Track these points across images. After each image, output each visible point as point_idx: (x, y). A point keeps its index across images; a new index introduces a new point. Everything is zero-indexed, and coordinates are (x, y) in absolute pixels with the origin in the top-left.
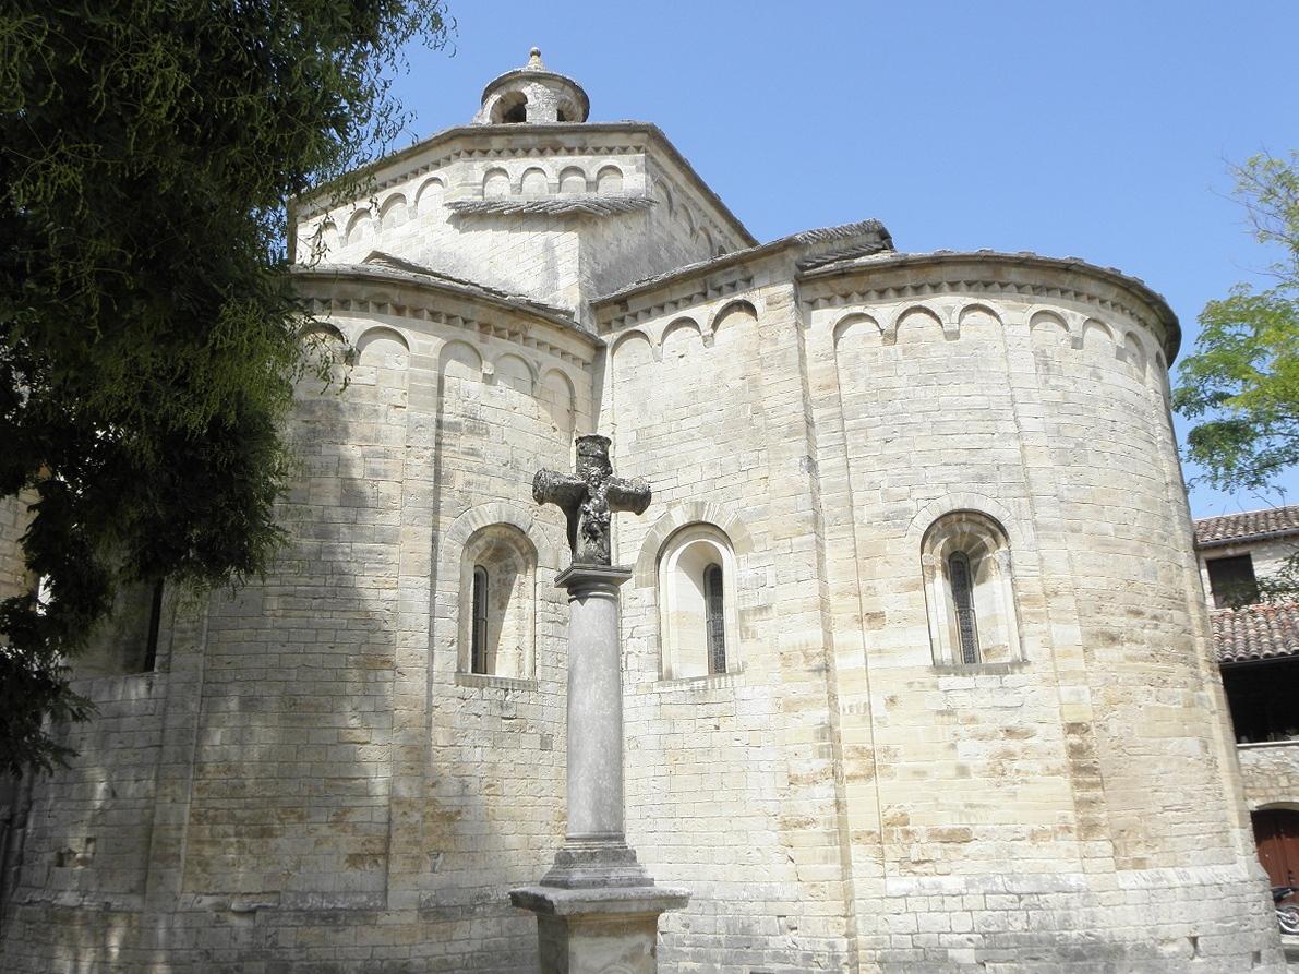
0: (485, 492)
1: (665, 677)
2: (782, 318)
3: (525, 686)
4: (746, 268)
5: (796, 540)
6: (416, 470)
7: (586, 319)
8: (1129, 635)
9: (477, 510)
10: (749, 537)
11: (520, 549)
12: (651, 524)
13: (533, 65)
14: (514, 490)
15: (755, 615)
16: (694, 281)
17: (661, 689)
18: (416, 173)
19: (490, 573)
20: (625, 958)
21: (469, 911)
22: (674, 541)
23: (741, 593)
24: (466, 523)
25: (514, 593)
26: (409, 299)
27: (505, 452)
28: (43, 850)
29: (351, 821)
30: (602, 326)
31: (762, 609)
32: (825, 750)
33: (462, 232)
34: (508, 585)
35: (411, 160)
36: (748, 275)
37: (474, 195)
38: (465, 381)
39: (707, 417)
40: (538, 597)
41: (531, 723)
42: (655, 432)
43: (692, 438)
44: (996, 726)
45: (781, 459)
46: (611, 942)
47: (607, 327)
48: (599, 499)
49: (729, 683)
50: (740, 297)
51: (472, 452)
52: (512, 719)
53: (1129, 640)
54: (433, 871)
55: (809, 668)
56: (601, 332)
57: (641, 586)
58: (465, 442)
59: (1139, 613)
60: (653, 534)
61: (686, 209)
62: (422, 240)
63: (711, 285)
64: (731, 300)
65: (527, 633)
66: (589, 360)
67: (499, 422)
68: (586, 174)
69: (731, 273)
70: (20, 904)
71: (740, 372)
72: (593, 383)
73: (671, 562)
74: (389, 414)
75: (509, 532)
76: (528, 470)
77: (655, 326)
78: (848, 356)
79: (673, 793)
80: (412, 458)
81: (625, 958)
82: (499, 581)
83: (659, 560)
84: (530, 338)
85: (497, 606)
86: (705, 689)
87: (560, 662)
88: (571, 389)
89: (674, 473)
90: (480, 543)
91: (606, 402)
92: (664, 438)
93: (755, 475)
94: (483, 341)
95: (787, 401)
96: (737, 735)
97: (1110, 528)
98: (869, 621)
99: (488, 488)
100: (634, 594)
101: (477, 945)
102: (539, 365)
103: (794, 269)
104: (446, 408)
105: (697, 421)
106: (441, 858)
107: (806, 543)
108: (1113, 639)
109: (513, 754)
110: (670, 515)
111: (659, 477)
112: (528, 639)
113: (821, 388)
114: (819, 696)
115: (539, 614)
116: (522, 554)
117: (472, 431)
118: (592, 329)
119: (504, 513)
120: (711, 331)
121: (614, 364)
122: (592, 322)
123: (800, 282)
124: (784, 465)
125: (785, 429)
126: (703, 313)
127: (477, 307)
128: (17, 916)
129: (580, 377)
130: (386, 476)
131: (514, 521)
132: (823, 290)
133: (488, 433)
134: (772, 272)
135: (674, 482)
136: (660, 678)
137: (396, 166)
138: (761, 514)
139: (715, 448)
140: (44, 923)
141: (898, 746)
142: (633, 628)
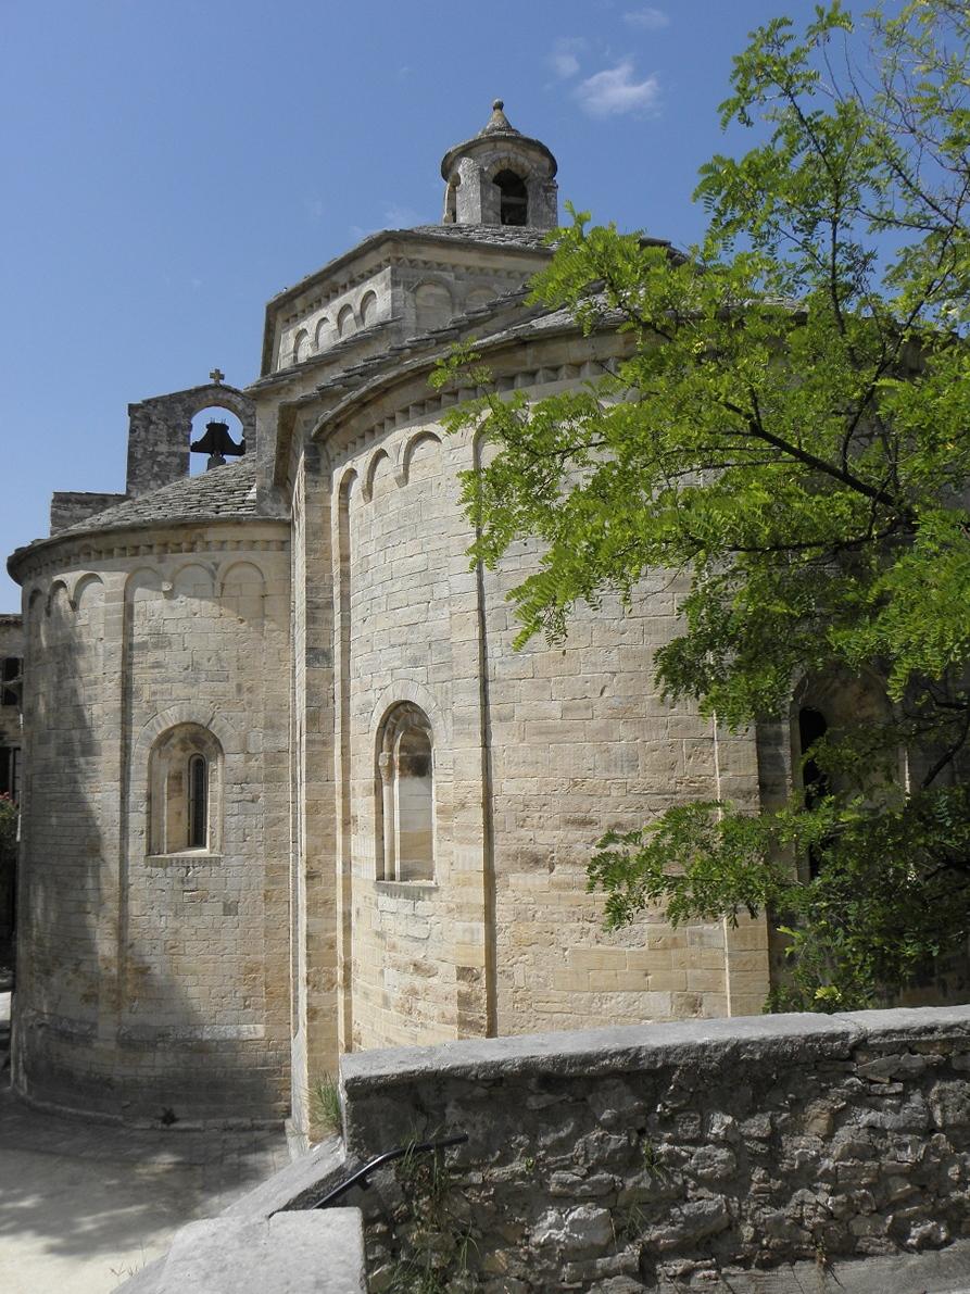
8: (563, 853)
14: (194, 690)
21: (152, 1045)
24: (153, 729)
26: (102, 543)
27: (185, 658)
38: (150, 603)
41: (212, 893)
44: (407, 959)
51: (157, 665)
53: (561, 861)
54: (131, 1012)
58: (152, 657)
59: (585, 823)
67: (179, 631)
90: (174, 741)
97: (555, 709)
101: (159, 1072)
102: (217, 565)
104: (136, 631)
106: (137, 1003)
108: (536, 861)
109: (194, 921)
117: (156, 646)
131: (194, 718)
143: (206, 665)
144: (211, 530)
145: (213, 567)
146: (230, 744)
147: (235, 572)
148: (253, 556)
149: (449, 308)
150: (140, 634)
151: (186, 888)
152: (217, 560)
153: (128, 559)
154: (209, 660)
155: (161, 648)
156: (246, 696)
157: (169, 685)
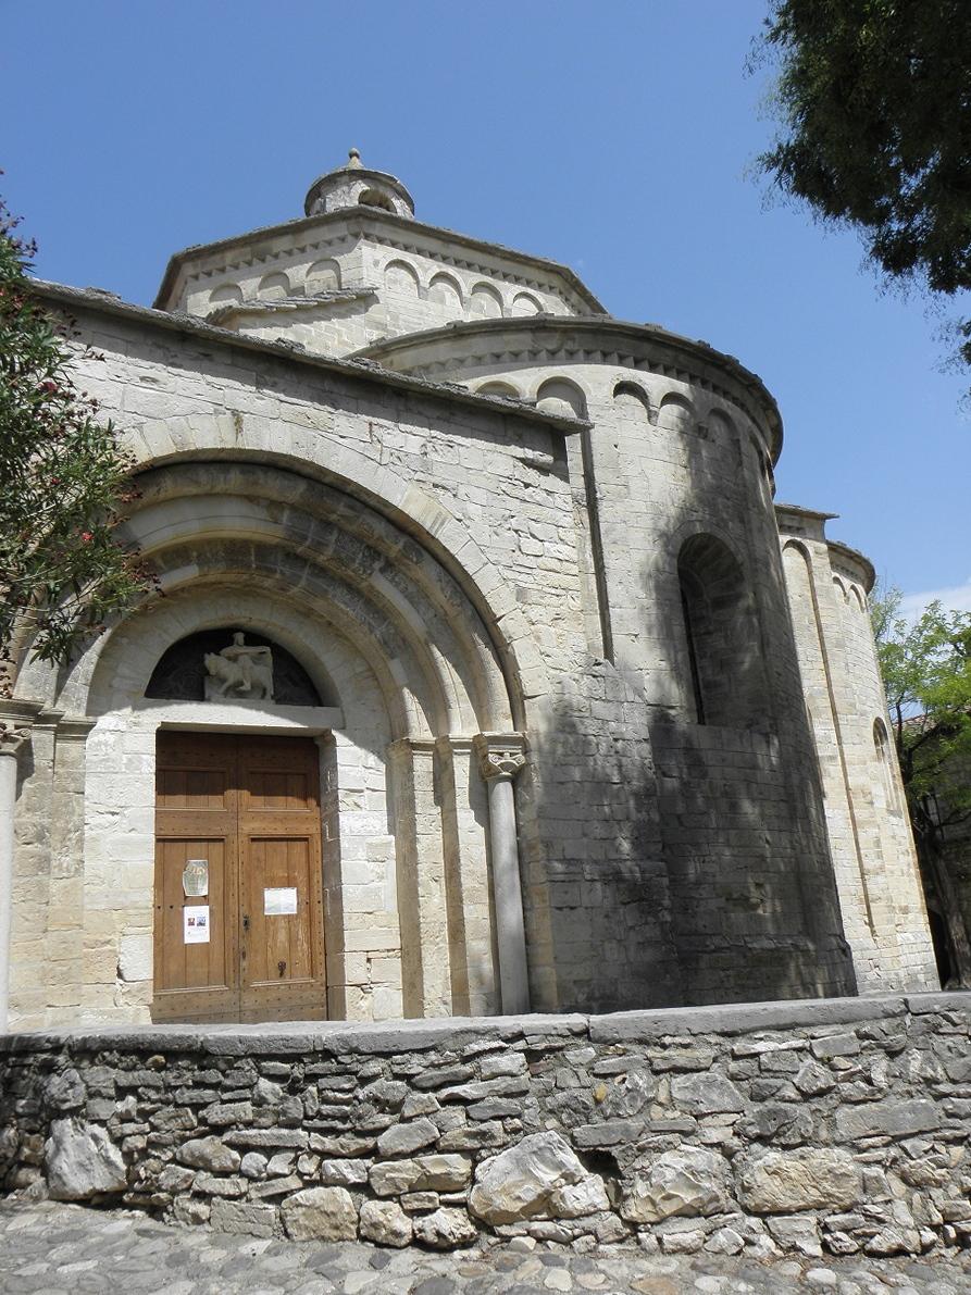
4: (802, 521)
13: (356, 164)
18: (482, 270)
28: (705, 896)
35: (507, 263)
70: (702, 952)
128: (703, 965)
137: (491, 257)
140: (745, 967)
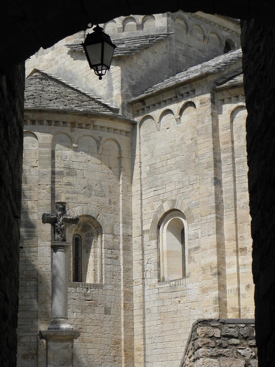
0: (75, 201)
1: (161, 280)
2: (206, 110)
3: (95, 286)
5: (209, 217)
6: (43, 195)
7: (126, 112)
9: (72, 210)
10: (193, 216)
11: (94, 226)
12: (156, 210)
14: (89, 199)
15: (194, 251)
16: (171, 91)
17: (159, 287)
19: (82, 237)
20: (64, 348)
22: (165, 219)
23: (189, 241)
25: (92, 246)
27: (84, 182)
29: (23, 341)
30: (135, 113)
31: (197, 248)
32: (217, 308)
33: (74, 60)
34: (89, 243)
36: (193, 89)
37: (80, 38)
39: (178, 159)
40: (103, 248)
42: (157, 166)
43: (171, 169)
45: (204, 179)
46: (60, 344)
47: (137, 114)
48: (60, 222)
49: (184, 282)
50: (189, 100)
51: (69, 184)
52: (90, 301)
55: (212, 273)
56: (134, 116)
57: (152, 240)
58: (65, 180)
60: (156, 215)
61: (200, 26)
62: (57, 63)
63: (179, 94)
64: (186, 101)
65: (98, 263)
66: (129, 130)
67: (81, 168)
68: (136, 20)
69: (186, 87)
71: (190, 136)
72: (132, 141)
73: (164, 228)
74: (31, 170)
75: (88, 219)
76: (96, 189)
77: (156, 113)
78: (237, 126)
79: (163, 332)
80: (41, 190)
81: (64, 348)
82: (86, 241)
83: (159, 227)
84: (96, 126)
85: (85, 252)
86: (175, 285)
87: (114, 276)
88: (119, 147)
89: (164, 186)
91: (137, 152)
92: (161, 169)
93: (195, 186)
94: (72, 131)
95: (207, 151)
96: (186, 305)
98: (241, 251)
99: (77, 200)
100: (149, 244)
102: (101, 138)
103: (212, 84)
104: (56, 165)
105: (173, 161)
107: (212, 218)
109: (91, 316)
110: (163, 206)
111: (160, 188)
112: (98, 266)
113: (225, 143)
114: (215, 285)
115: (103, 255)
116: (95, 228)
117: (68, 174)
118: (129, 116)
119: (85, 211)
120: (178, 116)
121: (141, 132)
122: (129, 111)
123: (214, 92)
124: (205, 182)
125: (206, 165)
126: (175, 107)
127: (69, 116)
129: (124, 140)
130: (30, 198)
131: (90, 214)
132: (226, 94)
133: (76, 174)
134: (202, 87)
135: (164, 191)
136: (159, 281)
138: (197, 204)
139: (180, 174)
141: (249, 306)
142: (148, 259)
143: (96, 188)
144: (99, 120)
145: (99, 139)
146: (106, 229)
147: (107, 143)
148: (117, 137)
149: (185, 32)
150: (59, 166)
151: (87, 298)
152: (101, 136)
153: (52, 127)
154: (96, 185)
155: (72, 175)
156: (112, 206)
157: (76, 196)
